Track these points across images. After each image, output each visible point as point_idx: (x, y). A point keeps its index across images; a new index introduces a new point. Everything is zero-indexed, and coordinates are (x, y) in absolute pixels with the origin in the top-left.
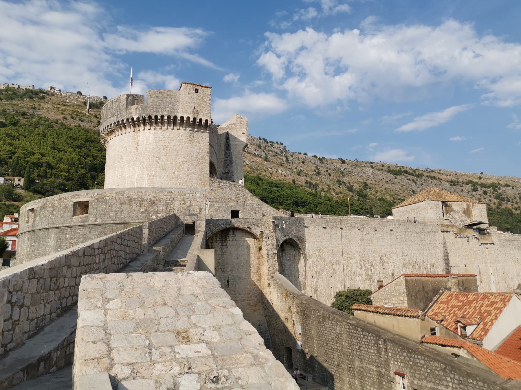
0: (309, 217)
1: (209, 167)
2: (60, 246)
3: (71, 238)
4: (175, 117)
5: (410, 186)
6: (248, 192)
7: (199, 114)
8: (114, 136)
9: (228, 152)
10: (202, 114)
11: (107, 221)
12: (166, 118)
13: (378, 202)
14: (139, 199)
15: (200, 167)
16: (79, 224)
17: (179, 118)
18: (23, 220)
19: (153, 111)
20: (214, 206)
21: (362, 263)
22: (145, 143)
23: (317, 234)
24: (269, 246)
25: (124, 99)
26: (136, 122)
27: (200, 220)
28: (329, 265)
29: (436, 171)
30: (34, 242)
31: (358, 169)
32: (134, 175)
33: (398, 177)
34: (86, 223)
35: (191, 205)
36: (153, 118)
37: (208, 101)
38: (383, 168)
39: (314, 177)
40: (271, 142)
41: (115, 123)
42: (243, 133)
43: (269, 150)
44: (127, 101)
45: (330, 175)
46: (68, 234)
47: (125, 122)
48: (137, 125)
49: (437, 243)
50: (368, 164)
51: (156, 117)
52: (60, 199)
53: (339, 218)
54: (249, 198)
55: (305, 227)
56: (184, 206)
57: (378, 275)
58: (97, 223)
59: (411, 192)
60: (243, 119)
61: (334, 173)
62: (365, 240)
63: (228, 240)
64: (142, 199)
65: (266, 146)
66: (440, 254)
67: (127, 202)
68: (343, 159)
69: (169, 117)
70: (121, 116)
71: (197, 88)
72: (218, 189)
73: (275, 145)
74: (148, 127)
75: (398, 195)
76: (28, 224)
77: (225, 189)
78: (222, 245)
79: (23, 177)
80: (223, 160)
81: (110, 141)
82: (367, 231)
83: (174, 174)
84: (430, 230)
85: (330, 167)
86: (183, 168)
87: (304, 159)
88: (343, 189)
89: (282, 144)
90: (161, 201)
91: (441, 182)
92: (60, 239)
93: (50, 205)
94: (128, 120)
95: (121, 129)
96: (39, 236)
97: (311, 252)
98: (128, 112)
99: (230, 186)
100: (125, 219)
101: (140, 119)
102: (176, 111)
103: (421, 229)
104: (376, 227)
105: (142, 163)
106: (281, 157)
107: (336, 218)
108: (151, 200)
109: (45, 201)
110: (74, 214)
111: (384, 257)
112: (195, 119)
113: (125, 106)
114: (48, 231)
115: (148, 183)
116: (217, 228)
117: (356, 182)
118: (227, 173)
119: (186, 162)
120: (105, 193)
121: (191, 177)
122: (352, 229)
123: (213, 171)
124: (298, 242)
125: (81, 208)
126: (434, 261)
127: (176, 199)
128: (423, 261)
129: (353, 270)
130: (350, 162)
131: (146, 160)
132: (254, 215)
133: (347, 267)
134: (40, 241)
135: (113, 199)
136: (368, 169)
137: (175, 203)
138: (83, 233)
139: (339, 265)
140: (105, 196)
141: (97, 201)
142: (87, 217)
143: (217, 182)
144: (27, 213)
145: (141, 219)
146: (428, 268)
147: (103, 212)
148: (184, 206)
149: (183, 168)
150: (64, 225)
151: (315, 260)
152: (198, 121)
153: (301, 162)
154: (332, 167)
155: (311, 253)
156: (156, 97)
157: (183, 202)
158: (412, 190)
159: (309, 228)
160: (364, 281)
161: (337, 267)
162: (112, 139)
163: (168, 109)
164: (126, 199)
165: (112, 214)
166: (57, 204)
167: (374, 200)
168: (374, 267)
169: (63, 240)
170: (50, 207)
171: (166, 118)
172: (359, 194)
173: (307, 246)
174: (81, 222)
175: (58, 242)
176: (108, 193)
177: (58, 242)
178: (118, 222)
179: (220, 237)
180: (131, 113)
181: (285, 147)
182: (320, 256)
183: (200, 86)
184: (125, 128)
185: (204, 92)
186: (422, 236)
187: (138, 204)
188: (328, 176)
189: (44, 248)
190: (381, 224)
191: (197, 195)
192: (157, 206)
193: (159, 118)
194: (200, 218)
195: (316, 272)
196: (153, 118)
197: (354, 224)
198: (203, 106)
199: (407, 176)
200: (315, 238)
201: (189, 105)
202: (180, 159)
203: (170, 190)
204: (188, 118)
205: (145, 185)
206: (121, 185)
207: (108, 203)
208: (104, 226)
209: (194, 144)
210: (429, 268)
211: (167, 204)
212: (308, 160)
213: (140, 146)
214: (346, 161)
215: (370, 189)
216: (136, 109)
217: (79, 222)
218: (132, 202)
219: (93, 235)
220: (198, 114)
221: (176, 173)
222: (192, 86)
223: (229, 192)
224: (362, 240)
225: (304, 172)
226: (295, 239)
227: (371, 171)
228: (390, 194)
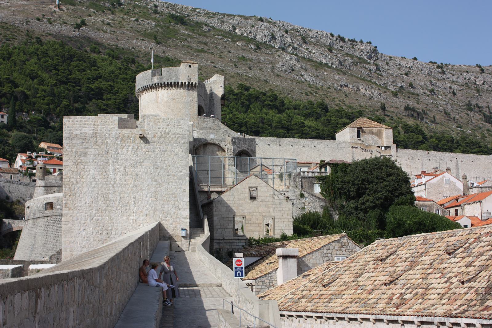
4: (178, 83)
6: (221, 123)
9: (211, 98)
17: (180, 83)
42: (221, 87)
43: (347, 54)
45: (454, 94)
49: (347, 155)
54: (222, 127)
55: (256, 144)
65: (342, 47)
68: (483, 65)
71: (190, 64)
74: (164, 88)
85: (458, 80)
87: (410, 68)
88: (476, 117)
95: (149, 90)
112: (189, 83)
113: (151, 77)
123: (200, 112)
124: (250, 152)
143: (202, 118)
154: (461, 81)
171: (173, 83)
181: (376, 47)
186: (337, 151)
188: (449, 96)
196: (166, 83)
223: (210, 124)
226: (248, 150)
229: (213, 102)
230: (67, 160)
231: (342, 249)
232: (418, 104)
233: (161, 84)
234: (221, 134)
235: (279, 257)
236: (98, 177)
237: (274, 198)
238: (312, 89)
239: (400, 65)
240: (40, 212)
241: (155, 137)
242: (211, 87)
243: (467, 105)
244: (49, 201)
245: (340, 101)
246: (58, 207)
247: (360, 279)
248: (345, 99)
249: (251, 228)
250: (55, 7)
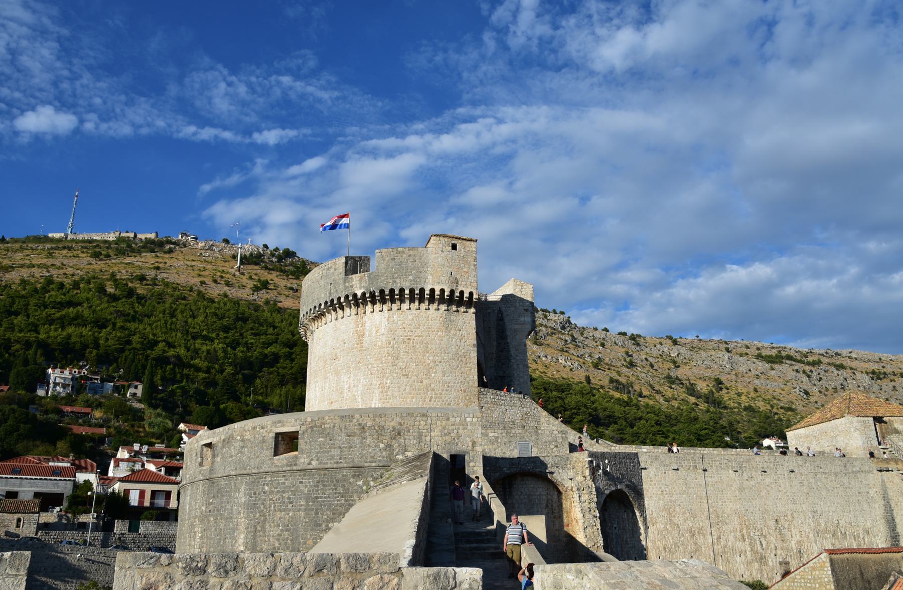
0: (645, 450)
1: (476, 370)
2: (254, 504)
3: (272, 492)
4: (422, 290)
5: (799, 382)
6: (540, 409)
7: (460, 283)
8: (324, 322)
10: (464, 283)
11: (327, 463)
12: (407, 292)
13: (744, 413)
14: (377, 428)
16: (284, 469)
17: (427, 292)
18: (193, 462)
19: (388, 282)
20: (487, 435)
21: (745, 531)
22: (374, 333)
23: (663, 482)
24: (584, 504)
25: (341, 264)
26: (360, 299)
27: (473, 461)
28: (687, 535)
29: (844, 355)
30: (214, 497)
31: (703, 354)
32: (357, 386)
33: (776, 366)
34: (295, 468)
35: (459, 437)
36: (387, 292)
37: (473, 263)
38: (748, 351)
39: (624, 370)
40: (543, 310)
41: (326, 303)
44: (346, 267)
46: (267, 485)
47: (342, 300)
48: (361, 305)
49: (872, 492)
50: (720, 345)
51: (392, 291)
52: (254, 428)
53: (698, 452)
54: (543, 420)
55: (642, 469)
56: (448, 438)
57: (774, 552)
58: (311, 467)
59: (802, 394)
60: (525, 287)
61: (658, 362)
62: (747, 491)
63: (514, 494)
64: (382, 428)
66: (879, 511)
67: (357, 431)
69: (412, 291)
70: (336, 291)
72: (492, 405)
73: (552, 316)
75: (779, 400)
76: (203, 468)
77: (503, 407)
79: (141, 382)
81: (316, 330)
82: (749, 474)
83: (422, 382)
84: (858, 469)
85: (652, 352)
86: (436, 372)
87: (604, 339)
89: (562, 313)
90: (411, 431)
91: (854, 374)
92: (255, 493)
93: (239, 438)
94: (347, 297)
96: (221, 488)
97: (655, 514)
98: (347, 284)
99: (511, 401)
100: (356, 460)
101: (367, 295)
102: (423, 281)
103: (843, 468)
104: (765, 466)
105: (370, 367)
106: (563, 337)
107: (692, 451)
108: (394, 428)
109: (230, 432)
110: (276, 454)
111: (782, 521)
112: (452, 292)
114: (236, 480)
115: (381, 399)
116: (497, 474)
117: (700, 378)
119: (440, 362)
120: (323, 418)
121: (448, 386)
122: (724, 472)
125: (286, 443)
126: (869, 524)
127: (434, 426)
128: (850, 524)
129: (730, 543)
130: (687, 341)
131: (376, 360)
132: (555, 449)
133: (719, 538)
134: (223, 496)
135: (336, 428)
136: (720, 354)
137: (433, 434)
138: (291, 483)
139: (704, 535)
140: (324, 424)
141: (312, 431)
142: (296, 457)
144: (199, 449)
145: (380, 461)
146: (859, 537)
147: (321, 448)
148: (448, 438)
149: (436, 372)
150: (262, 470)
151: (662, 527)
152: (457, 294)
153: (598, 343)
154: (655, 352)
156: (392, 259)
157: (446, 431)
158: (804, 390)
159: (648, 470)
160: (749, 563)
161: (701, 540)
162: (320, 328)
163: (410, 277)
164: (356, 427)
165: (335, 452)
166: (249, 437)
167: (736, 410)
168: (765, 537)
169: (259, 494)
170: (238, 441)
171: (407, 292)
172: (709, 398)
174: (287, 465)
175: (251, 497)
176: (327, 418)
177: (251, 497)
178: (345, 465)
179: (501, 489)
180: (352, 286)
181: (569, 317)
182: (671, 520)
183: (460, 239)
184: (342, 308)
185: (467, 248)
186: (846, 480)
187: (375, 436)
188: (648, 367)
189: (229, 507)
190: (772, 460)
191: (468, 419)
192: (405, 439)
193: (397, 292)
194: (473, 457)
195: (665, 548)
196: (387, 292)
197: (725, 461)
198: (465, 270)
199: (791, 365)
200: (660, 488)
201: (443, 269)
202: (431, 358)
203: (425, 412)
205: (375, 403)
206: (335, 402)
207: (328, 433)
208: (322, 473)
209: (452, 332)
210: (861, 537)
211: (420, 437)
212: (610, 339)
213: (366, 339)
214: (679, 340)
215: (728, 389)
216: (361, 279)
217: (282, 466)
218: (365, 432)
219: (306, 486)
220: (457, 283)
221: (424, 381)
222: (446, 239)
223: (510, 412)
224: (741, 489)
225: (605, 362)
227: (726, 357)
228: (764, 399)
232: (620, 376)
233: (373, 295)
234: (550, 443)
239: (593, 336)
243: (666, 377)
245: (541, 372)
248: (546, 371)
250: (236, 271)
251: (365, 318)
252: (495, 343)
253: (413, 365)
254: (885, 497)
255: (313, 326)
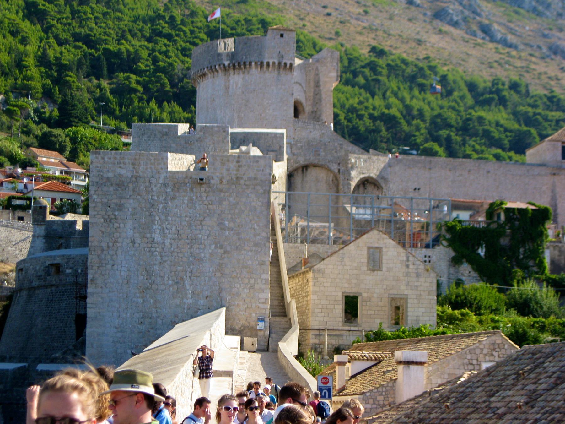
15: (285, 108)
49: (544, 188)
78: (303, 180)
80: (312, 98)
83: (261, 115)
86: (269, 110)
108: (241, 139)
112: (280, 63)
118: (316, 112)
149: (269, 110)
155: (396, 193)
163: (256, 55)
173: (391, 186)
180: (222, 59)
204: (274, 63)
209: (279, 86)
221: (263, 115)
229: (321, 95)
230: (95, 215)
231: (494, 353)
234: (332, 150)
235: (399, 363)
236: (138, 241)
237: (407, 266)
238: (503, 56)
240: (39, 277)
241: (221, 182)
242: (317, 69)
244: (55, 262)
245: (550, 78)
246: (68, 271)
247: (492, 399)
249: (369, 312)
251: (230, 78)
252: (313, 90)
253: (256, 105)
254: (553, 191)
255: (200, 80)
